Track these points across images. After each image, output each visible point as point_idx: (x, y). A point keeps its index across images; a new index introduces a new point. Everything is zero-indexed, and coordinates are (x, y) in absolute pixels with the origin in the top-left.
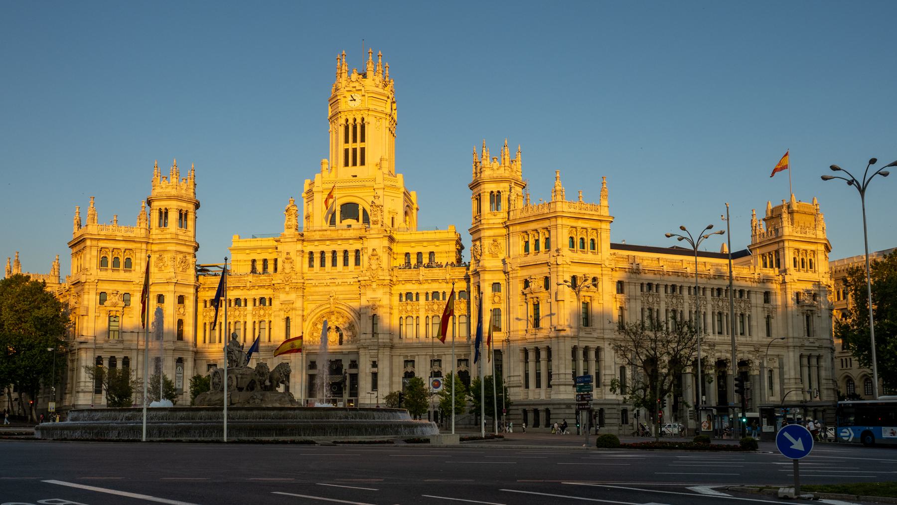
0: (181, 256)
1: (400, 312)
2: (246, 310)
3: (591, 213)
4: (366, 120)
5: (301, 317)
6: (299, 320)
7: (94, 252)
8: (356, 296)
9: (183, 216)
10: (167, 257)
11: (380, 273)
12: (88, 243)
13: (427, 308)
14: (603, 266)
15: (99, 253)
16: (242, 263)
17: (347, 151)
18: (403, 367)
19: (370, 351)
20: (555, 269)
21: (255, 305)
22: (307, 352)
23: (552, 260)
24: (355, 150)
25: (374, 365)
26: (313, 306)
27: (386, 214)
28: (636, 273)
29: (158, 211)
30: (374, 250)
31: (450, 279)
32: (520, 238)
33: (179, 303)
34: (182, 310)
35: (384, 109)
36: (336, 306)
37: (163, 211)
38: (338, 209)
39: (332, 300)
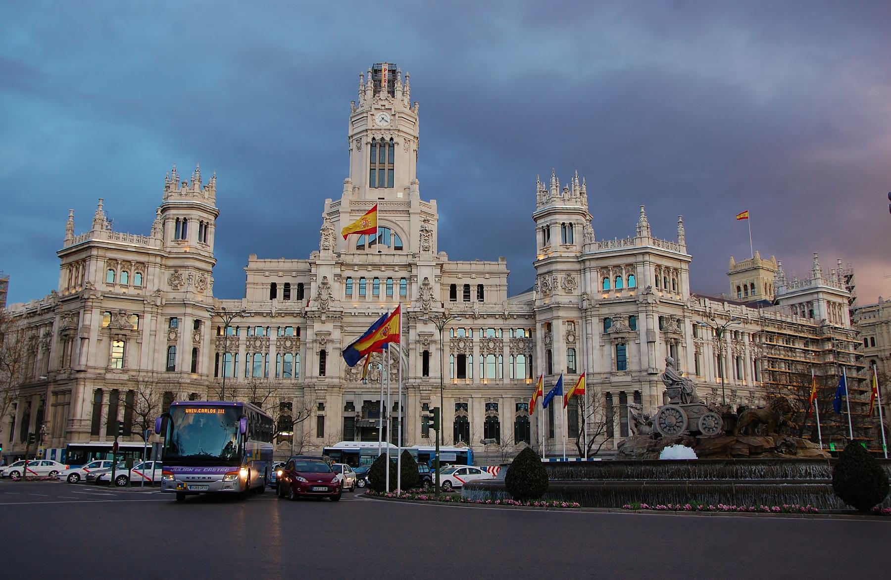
0: (197, 275)
2: (268, 340)
4: (395, 141)
7: (101, 264)
10: (185, 273)
11: (432, 304)
14: (686, 307)
15: (106, 264)
16: (258, 287)
19: (421, 392)
20: (644, 309)
22: (344, 390)
28: (707, 316)
29: (175, 221)
32: (599, 274)
33: (194, 329)
34: (197, 338)
35: (411, 132)
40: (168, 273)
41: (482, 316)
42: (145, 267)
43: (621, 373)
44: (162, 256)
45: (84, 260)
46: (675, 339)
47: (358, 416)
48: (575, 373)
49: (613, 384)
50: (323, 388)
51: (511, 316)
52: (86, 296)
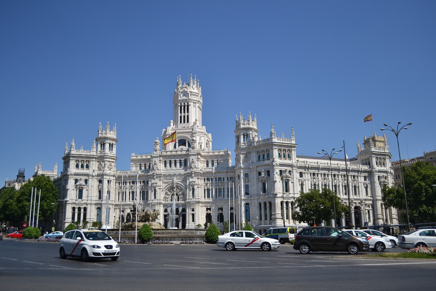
3: (287, 142)
4: (189, 104)
9: (111, 146)
13: (216, 184)
17: (181, 117)
24: (184, 116)
25: (193, 210)
27: (197, 143)
30: (193, 159)
31: (226, 172)
35: (197, 99)
38: (177, 141)
40: (97, 164)
46: (288, 179)
50: (155, 204)
52: (68, 174)
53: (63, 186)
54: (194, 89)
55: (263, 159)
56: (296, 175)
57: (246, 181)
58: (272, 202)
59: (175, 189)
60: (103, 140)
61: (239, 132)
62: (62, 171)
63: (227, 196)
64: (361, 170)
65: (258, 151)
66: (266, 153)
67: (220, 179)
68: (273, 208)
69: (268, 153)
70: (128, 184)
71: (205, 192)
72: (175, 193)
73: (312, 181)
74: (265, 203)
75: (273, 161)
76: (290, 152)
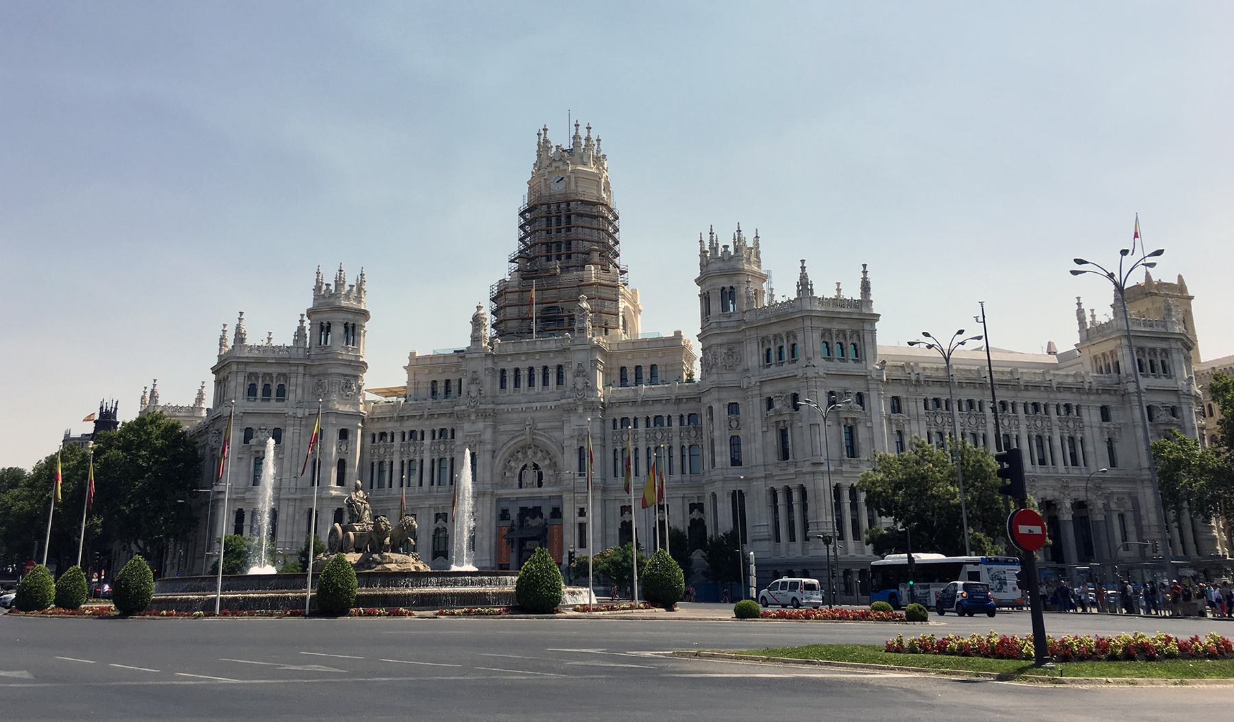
1: (614, 443)
5: (491, 453)
6: (488, 456)
7: (241, 379)
8: (558, 424)
12: (234, 368)
14: (869, 378)
18: (620, 515)
21: (434, 438)
23: (800, 373)
25: (582, 513)
26: (505, 438)
28: (915, 385)
29: (319, 326)
33: (340, 439)
34: (344, 448)
36: (534, 437)
37: (325, 325)
39: (528, 428)
41: (645, 402)
42: (287, 378)
43: (784, 463)
44: (305, 366)
45: (228, 377)
46: (854, 419)
47: (513, 525)
48: (741, 465)
49: (776, 478)
51: (678, 401)
53: (213, 449)
54: (585, 164)
55: (780, 359)
56: (880, 406)
57: (730, 426)
58: (809, 488)
59: (530, 452)
60: (325, 316)
61: (708, 283)
62: (211, 407)
63: (680, 470)
64: (1089, 389)
65: (763, 338)
66: (788, 341)
67: (658, 419)
68: (811, 506)
69: (792, 342)
70: (398, 439)
71: (615, 459)
72: (530, 464)
73: (930, 425)
74: (788, 492)
75: (806, 366)
76: (859, 340)
